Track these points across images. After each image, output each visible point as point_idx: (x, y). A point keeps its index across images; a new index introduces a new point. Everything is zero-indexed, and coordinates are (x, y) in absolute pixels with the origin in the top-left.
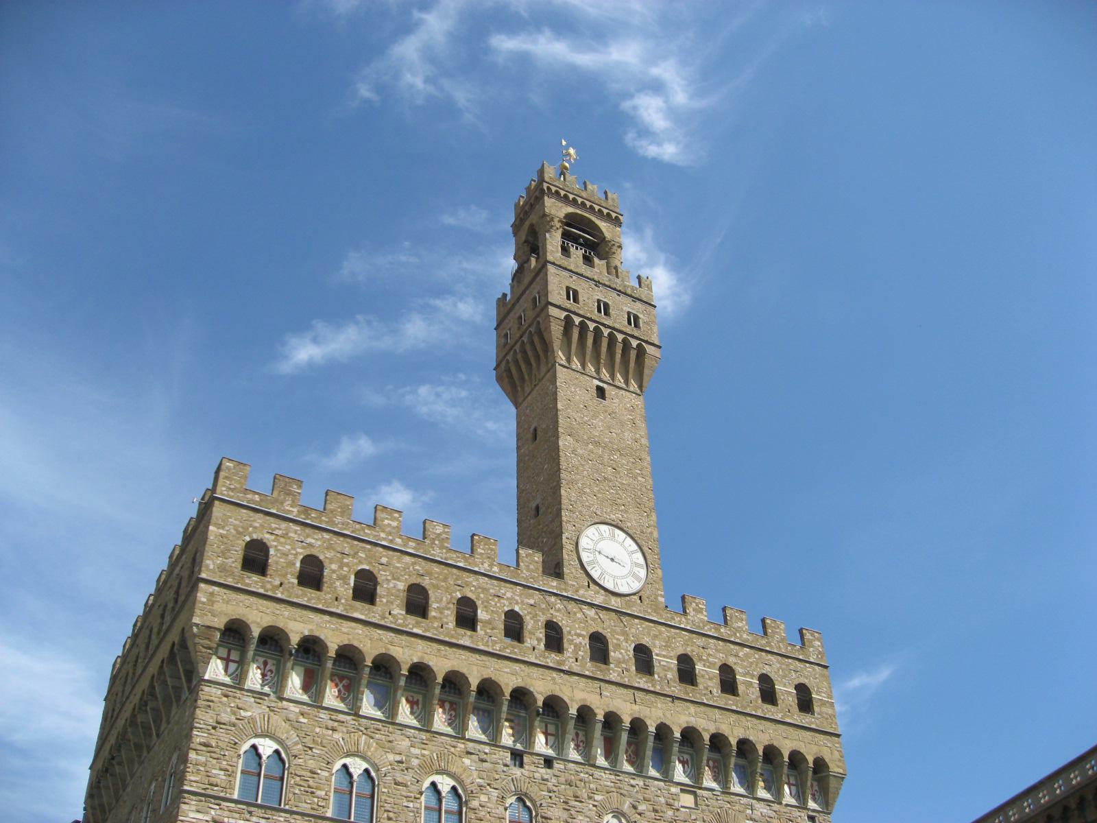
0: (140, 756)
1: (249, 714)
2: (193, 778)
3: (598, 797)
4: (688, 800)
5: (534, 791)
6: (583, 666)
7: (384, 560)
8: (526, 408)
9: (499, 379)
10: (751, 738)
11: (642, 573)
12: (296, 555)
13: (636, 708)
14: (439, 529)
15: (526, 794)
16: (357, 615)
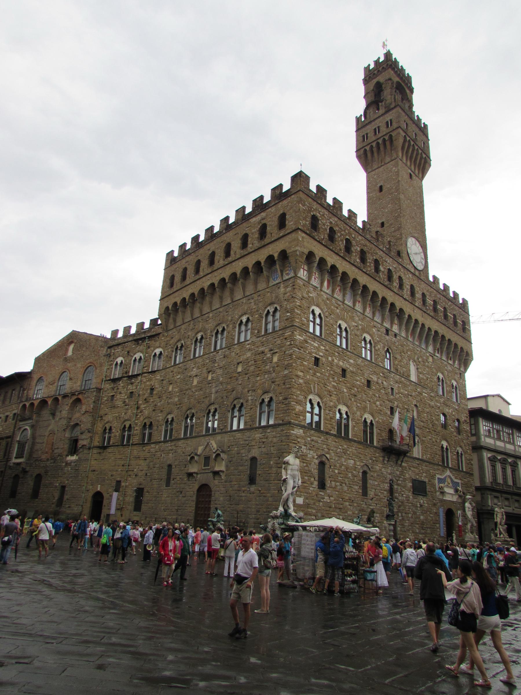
0: (221, 302)
1: (312, 295)
2: (297, 321)
3: (409, 353)
4: (430, 359)
5: (392, 346)
6: (409, 297)
7: (353, 236)
8: (375, 175)
9: (359, 157)
10: (451, 339)
11: (424, 263)
12: (327, 226)
13: (423, 319)
14: (368, 227)
15: (390, 347)
16: (347, 258)
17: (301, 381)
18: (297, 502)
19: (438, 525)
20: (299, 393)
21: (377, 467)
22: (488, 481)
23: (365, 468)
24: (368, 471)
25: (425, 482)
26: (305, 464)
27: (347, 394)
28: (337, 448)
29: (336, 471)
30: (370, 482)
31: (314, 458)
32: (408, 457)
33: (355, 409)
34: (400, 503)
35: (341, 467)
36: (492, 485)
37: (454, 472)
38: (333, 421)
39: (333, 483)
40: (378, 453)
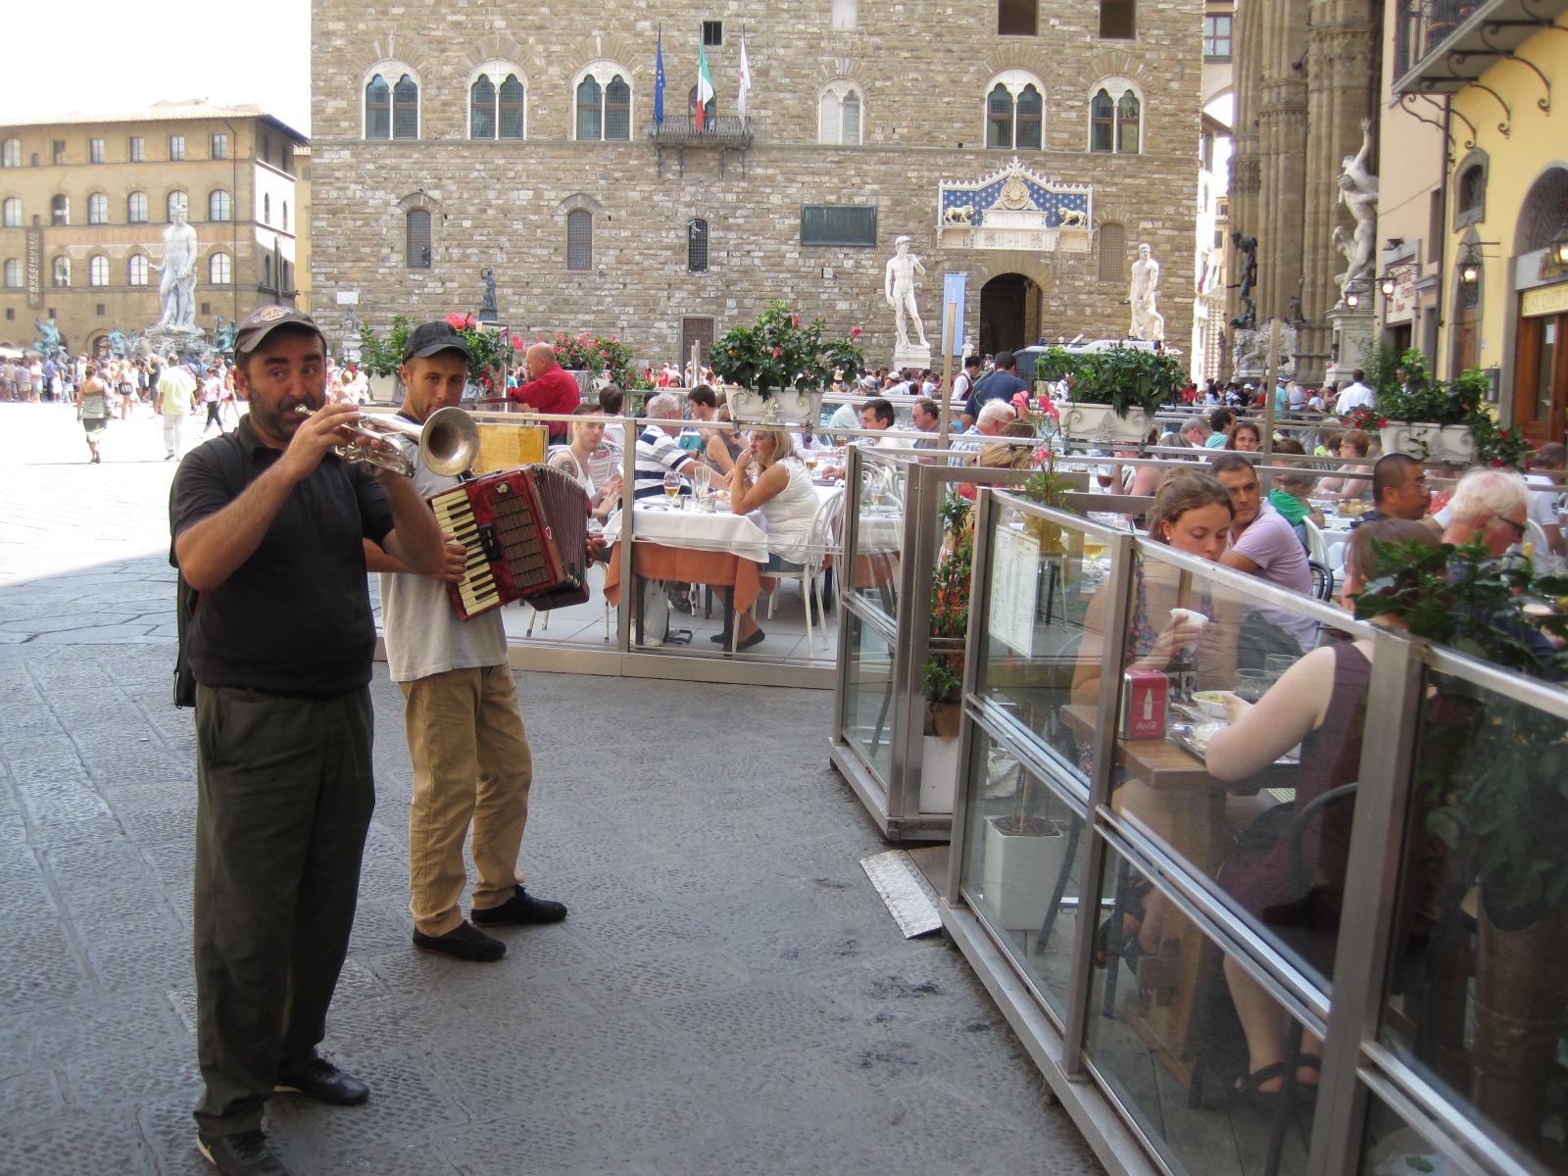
17: (339, 42)
18: (340, 301)
20: (331, 71)
21: (630, 194)
23: (580, 203)
24: (590, 208)
25: (871, 209)
26: (360, 223)
27: (508, 32)
28: (470, 170)
29: (467, 224)
30: (600, 234)
31: (387, 204)
32: (781, 149)
33: (539, 62)
34: (736, 275)
35: (485, 211)
37: (1056, 164)
38: (453, 109)
39: (456, 252)
40: (641, 157)
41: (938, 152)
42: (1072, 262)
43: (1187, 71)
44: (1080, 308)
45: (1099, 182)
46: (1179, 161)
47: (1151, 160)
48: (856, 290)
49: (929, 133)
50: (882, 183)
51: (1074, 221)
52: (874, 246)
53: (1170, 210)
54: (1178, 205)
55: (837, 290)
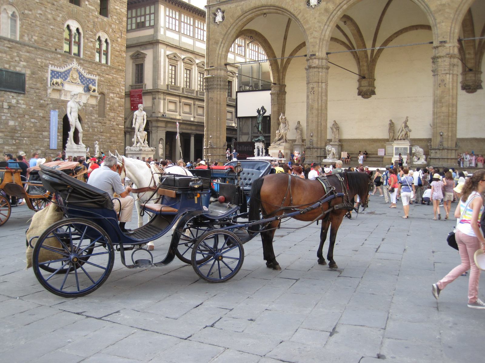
19: (45, 134)
22: (162, 83)
25: (24, 75)
36: (168, 88)
41: (49, 51)
42: (91, 108)
43: (123, 35)
44: (93, 127)
45: (99, 75)
46: (121, 70)
47: (113, 68)
48: (17, 115)
49: (45, 42)
50: (27, 62)
51: (94, 91)
52: (24, 94)
53: (118, 90)
54: (120, 88)
55: (9, 115)
